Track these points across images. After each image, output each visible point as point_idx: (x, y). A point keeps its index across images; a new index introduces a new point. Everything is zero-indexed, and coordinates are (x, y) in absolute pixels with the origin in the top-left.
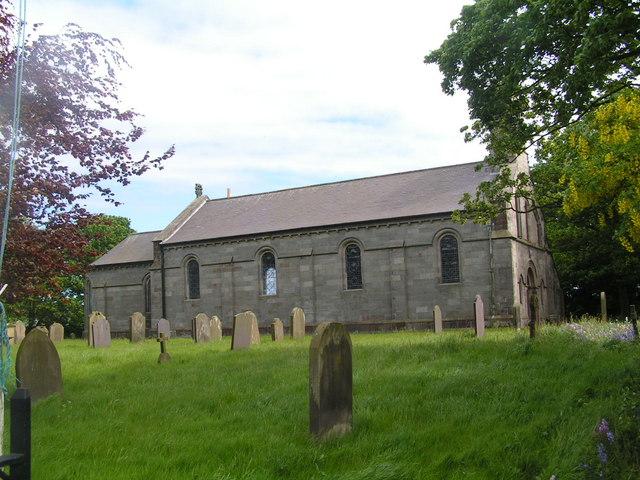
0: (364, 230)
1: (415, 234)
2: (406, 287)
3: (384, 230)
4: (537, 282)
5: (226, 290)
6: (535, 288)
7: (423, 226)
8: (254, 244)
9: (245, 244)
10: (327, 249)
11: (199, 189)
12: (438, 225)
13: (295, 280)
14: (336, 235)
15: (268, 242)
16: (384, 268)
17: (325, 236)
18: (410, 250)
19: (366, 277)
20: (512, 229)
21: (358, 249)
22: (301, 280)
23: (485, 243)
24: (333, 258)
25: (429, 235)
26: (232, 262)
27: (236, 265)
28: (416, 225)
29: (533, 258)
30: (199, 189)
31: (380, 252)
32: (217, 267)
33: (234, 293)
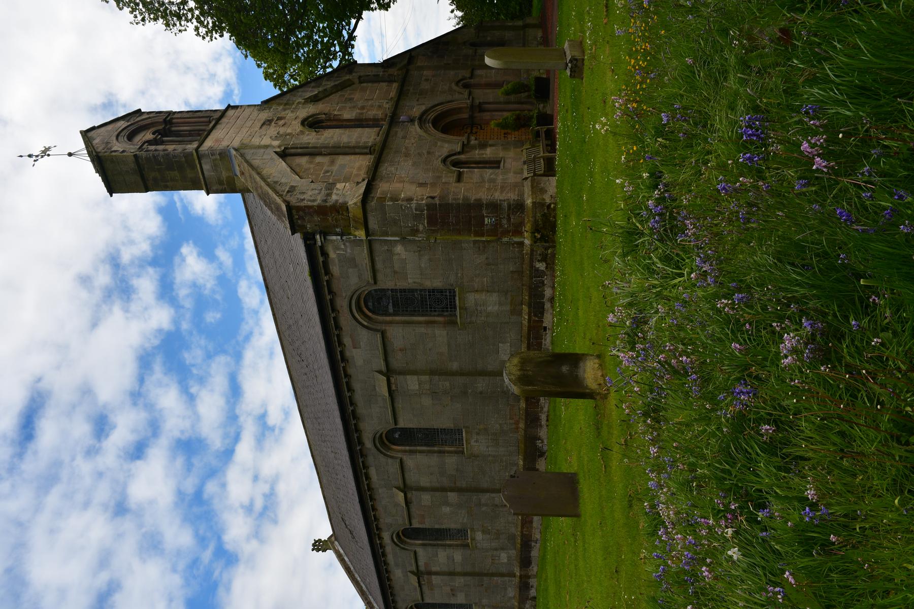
0: (362, 426)
1: (362, 352)
2: (461, 373)
3: (359, 396)
4: (461, 99)
5: (459, 581)
6: (472, 107)
7: (347, 340)
8: (389, 548)
9: (390, 558)
10: (393, 468)
11: (319, 546)
12: (345, 320)
13: (446, 510)
14: (370, 460)
15: (386, 536)
16: (427, 401)
17: (373, 472)
18: (397, 362)
19: (444, 422)
20: (349, 193)
21: (393, 431)
22: (446, 503)
23: (377, 247)
24: (410, 462)
25: (364, 335)
26: (418, 574)
27: (422, 568)
28: (348, 354)
29: (417, 111)
30: (319, 546)
31: (399, 405)
32: (425, 588)
33: (465, 574)
